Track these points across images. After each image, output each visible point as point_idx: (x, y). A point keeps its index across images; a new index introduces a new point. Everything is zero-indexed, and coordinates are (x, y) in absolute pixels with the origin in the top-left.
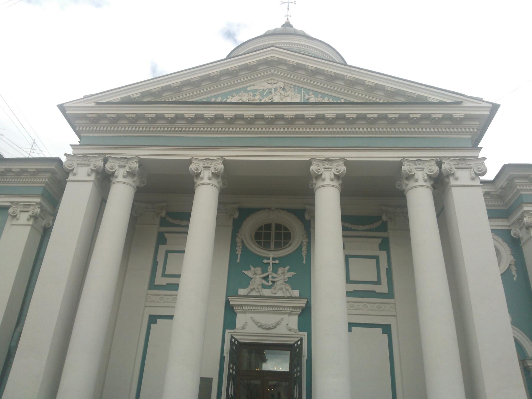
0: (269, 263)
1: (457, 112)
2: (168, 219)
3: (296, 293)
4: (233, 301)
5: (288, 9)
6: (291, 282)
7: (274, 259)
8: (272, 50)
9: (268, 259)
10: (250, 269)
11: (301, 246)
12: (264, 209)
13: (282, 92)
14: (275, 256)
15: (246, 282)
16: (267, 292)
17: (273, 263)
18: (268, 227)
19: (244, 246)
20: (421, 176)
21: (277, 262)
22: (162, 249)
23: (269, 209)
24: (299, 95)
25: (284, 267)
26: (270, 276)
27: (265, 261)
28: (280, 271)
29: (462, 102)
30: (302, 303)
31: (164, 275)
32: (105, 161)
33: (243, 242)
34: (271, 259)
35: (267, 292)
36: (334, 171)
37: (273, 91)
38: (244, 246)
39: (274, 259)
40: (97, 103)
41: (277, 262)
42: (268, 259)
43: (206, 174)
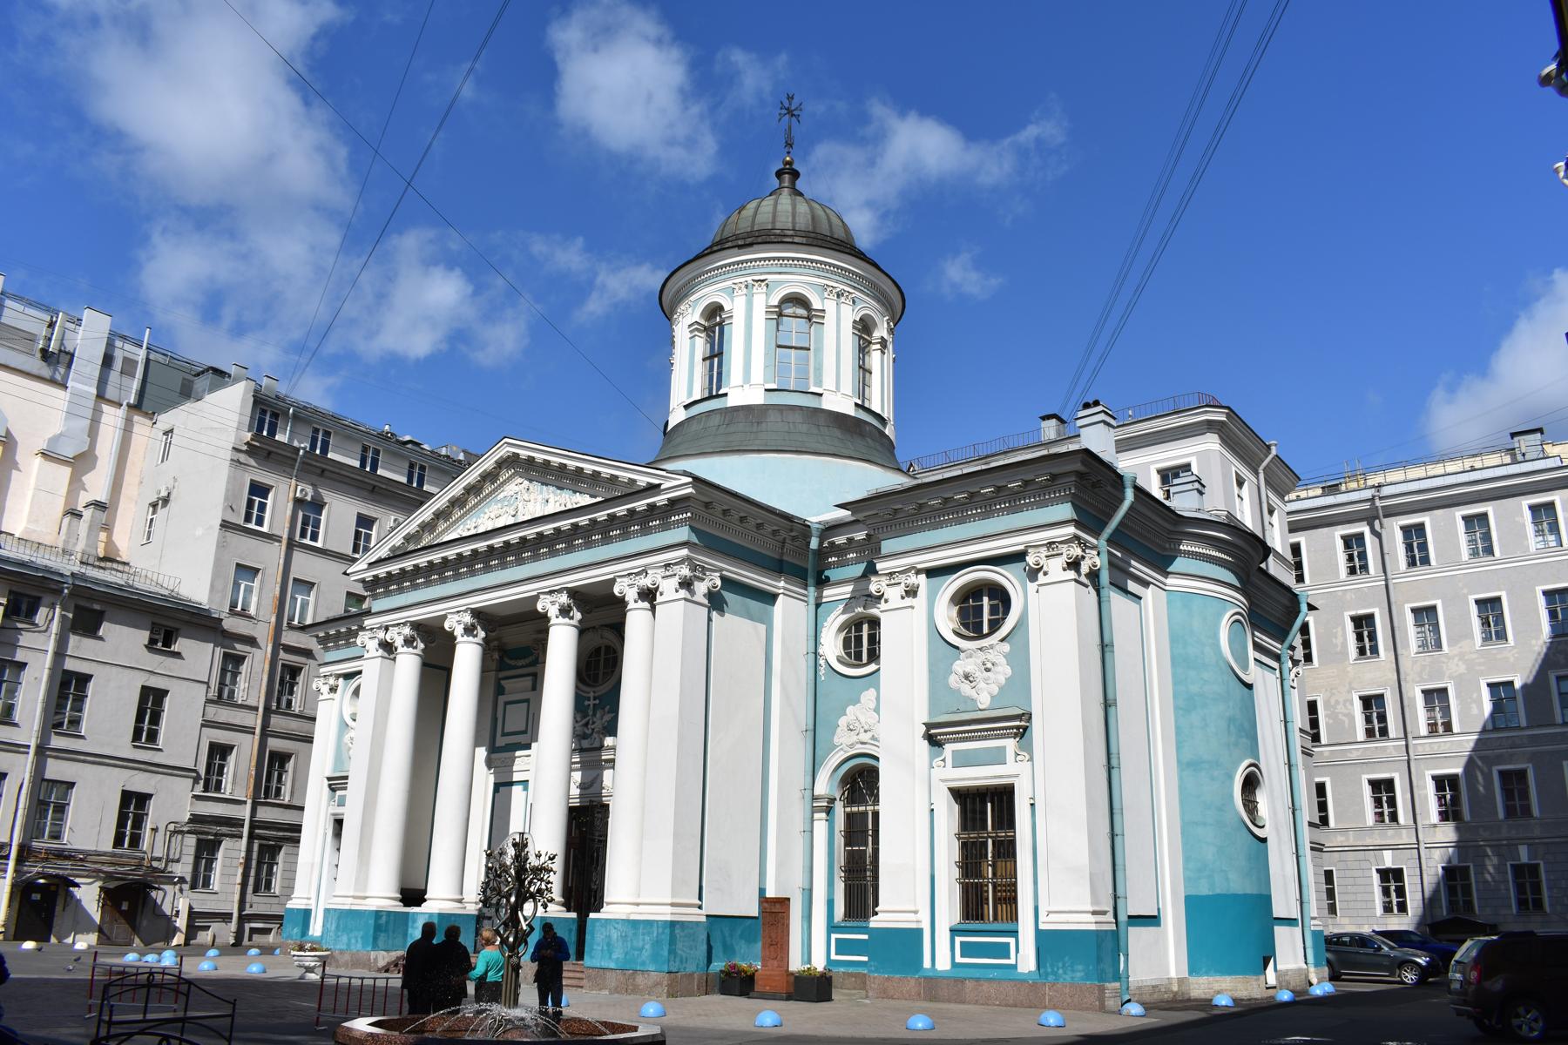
0: (589, 705)
1: (660, 500)
2: (507, 660)
8: (506, 443)
12: (588, 629)
14: (596, 695)
17: (594, 705)
20: (631, 595)
21: (597, 702)
22: (502, 699)
23: (594, 628)
26: (591, 722)
27: (586, 703)
29: (660, 485)
31: (504, 734)
32: (387, 629)
34: (592, 698)
39: (595, 699)
40: (370, 564)
41: (597, 702)
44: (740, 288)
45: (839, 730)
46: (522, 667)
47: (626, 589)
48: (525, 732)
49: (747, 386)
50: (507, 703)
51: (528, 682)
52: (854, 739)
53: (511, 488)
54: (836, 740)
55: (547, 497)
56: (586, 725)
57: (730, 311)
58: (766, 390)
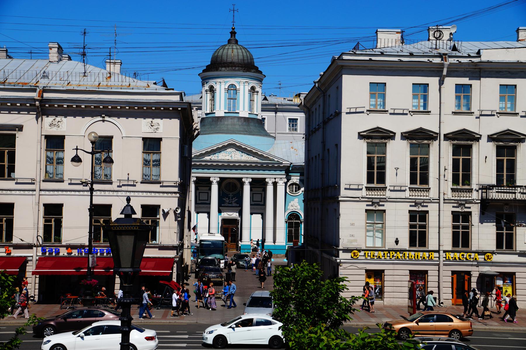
3: (238, 205)
4: (220, 208)
5: (234, 16)
6: (236, 202)
7: (232, 195)
9: (230, 195)
10: (225, 198)
11: (239, 191)
13: (235, 153)
15: (224, 202)
16: (230, 205)
18: (230, 183)
19: (222, 190)
22: (198, 192)
24: (239, 154)
25: (234, 197)
28: (234, 199)
30: (240, 208)
33: (222, 189)
35: (230, 205)
36: (248, 181)
37: (232, 152)
38: (222, 190)
39: (232, 195)
42: (230, 195)
43: (215, 181)
44: (242, 83)
45: (289, 206)
46: (204, 184)
47: (270, 181)
48: (208, 200)
49: (244, 111)
50: (199, 193)
51: (208, 188)
52: (293, 208)
53: (229, 150)
54: (288, 208)
55: (242, 155)
56: (230, 201)
57: (239, 89)
58: (249, 114)
